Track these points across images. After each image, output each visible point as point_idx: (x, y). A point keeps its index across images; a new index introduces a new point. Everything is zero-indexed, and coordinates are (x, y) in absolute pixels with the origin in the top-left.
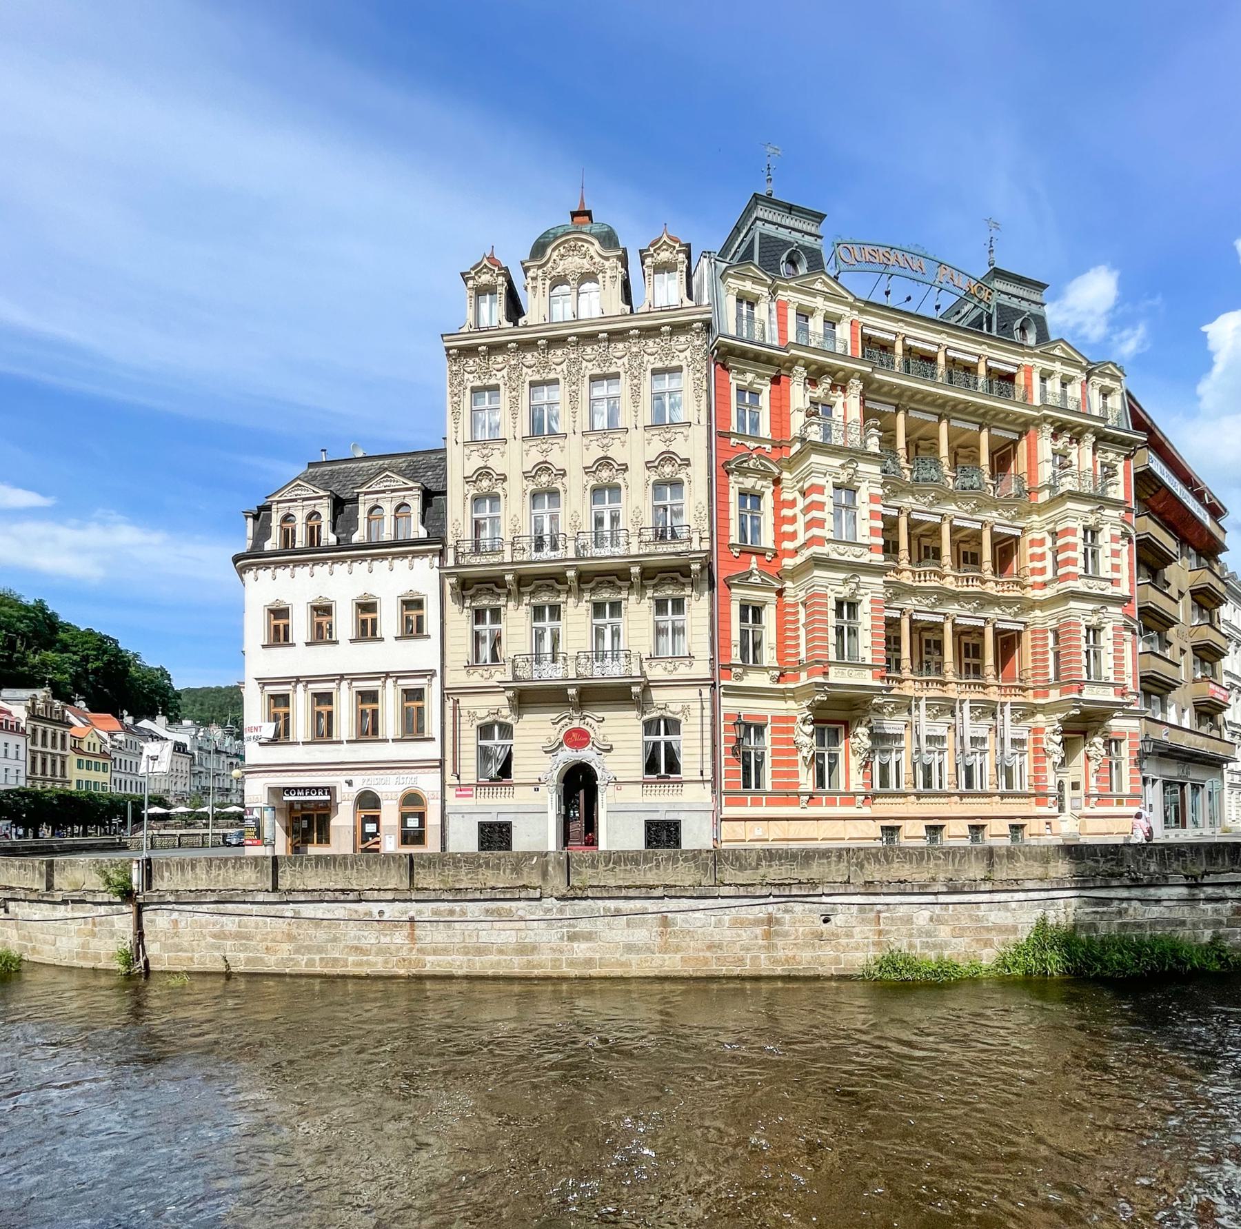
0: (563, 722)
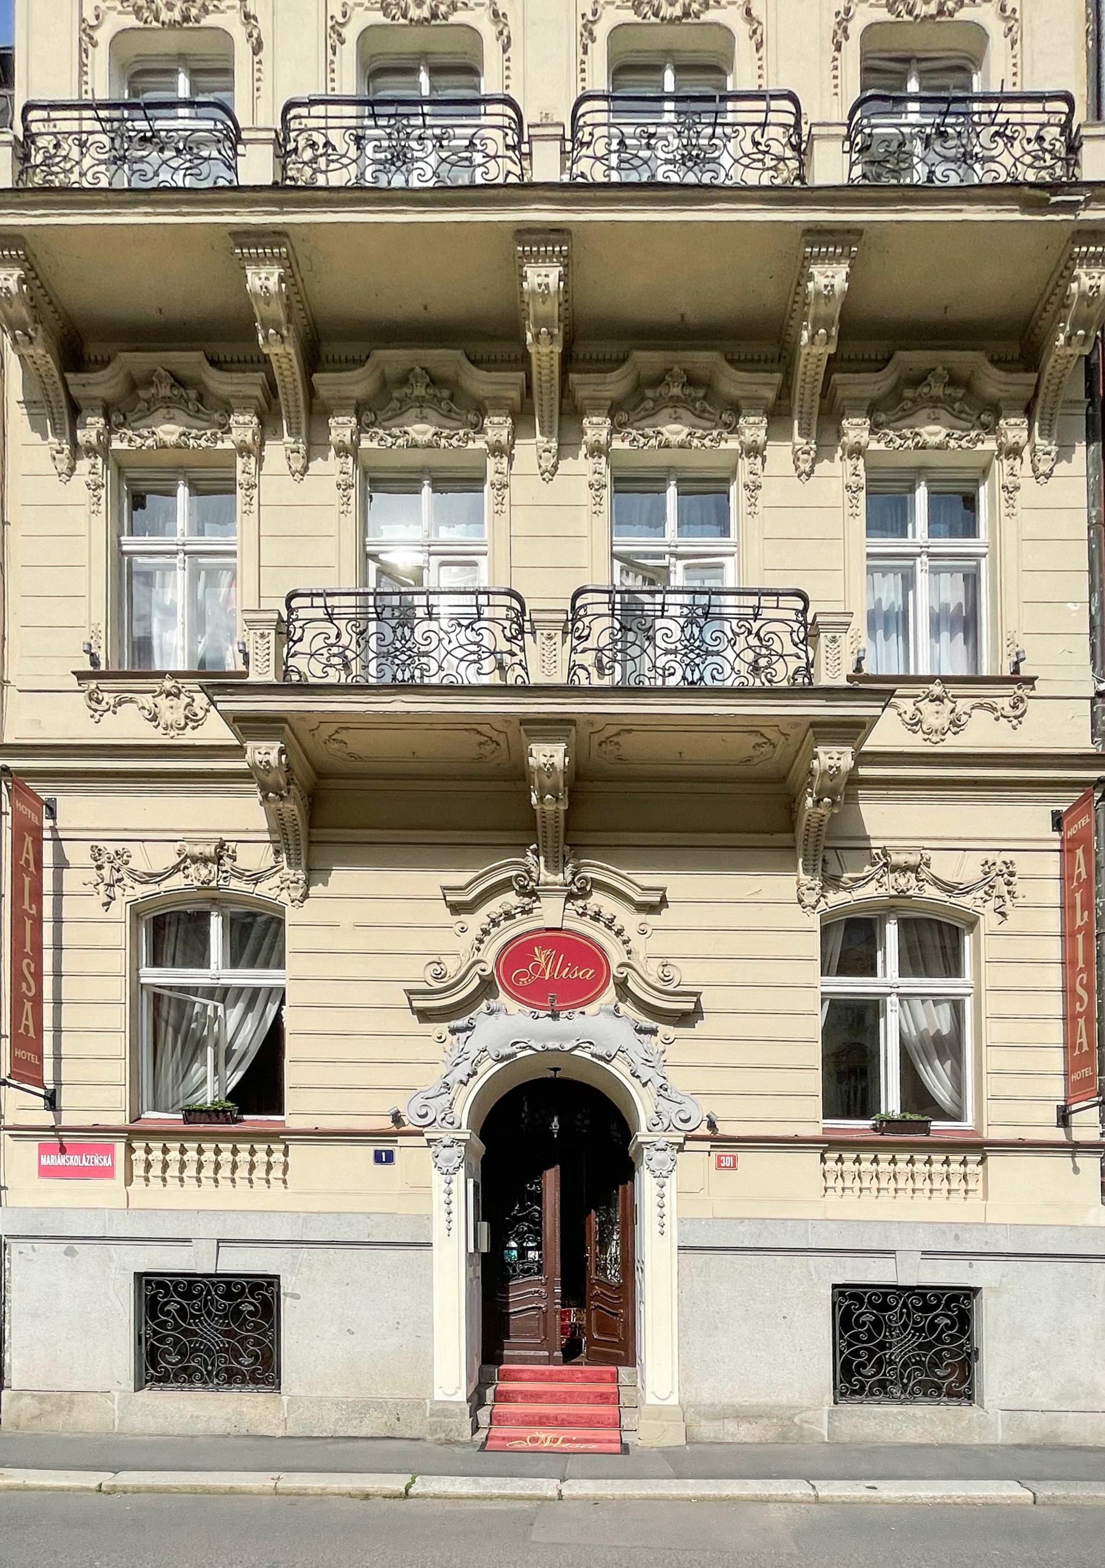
0: (494, 906)
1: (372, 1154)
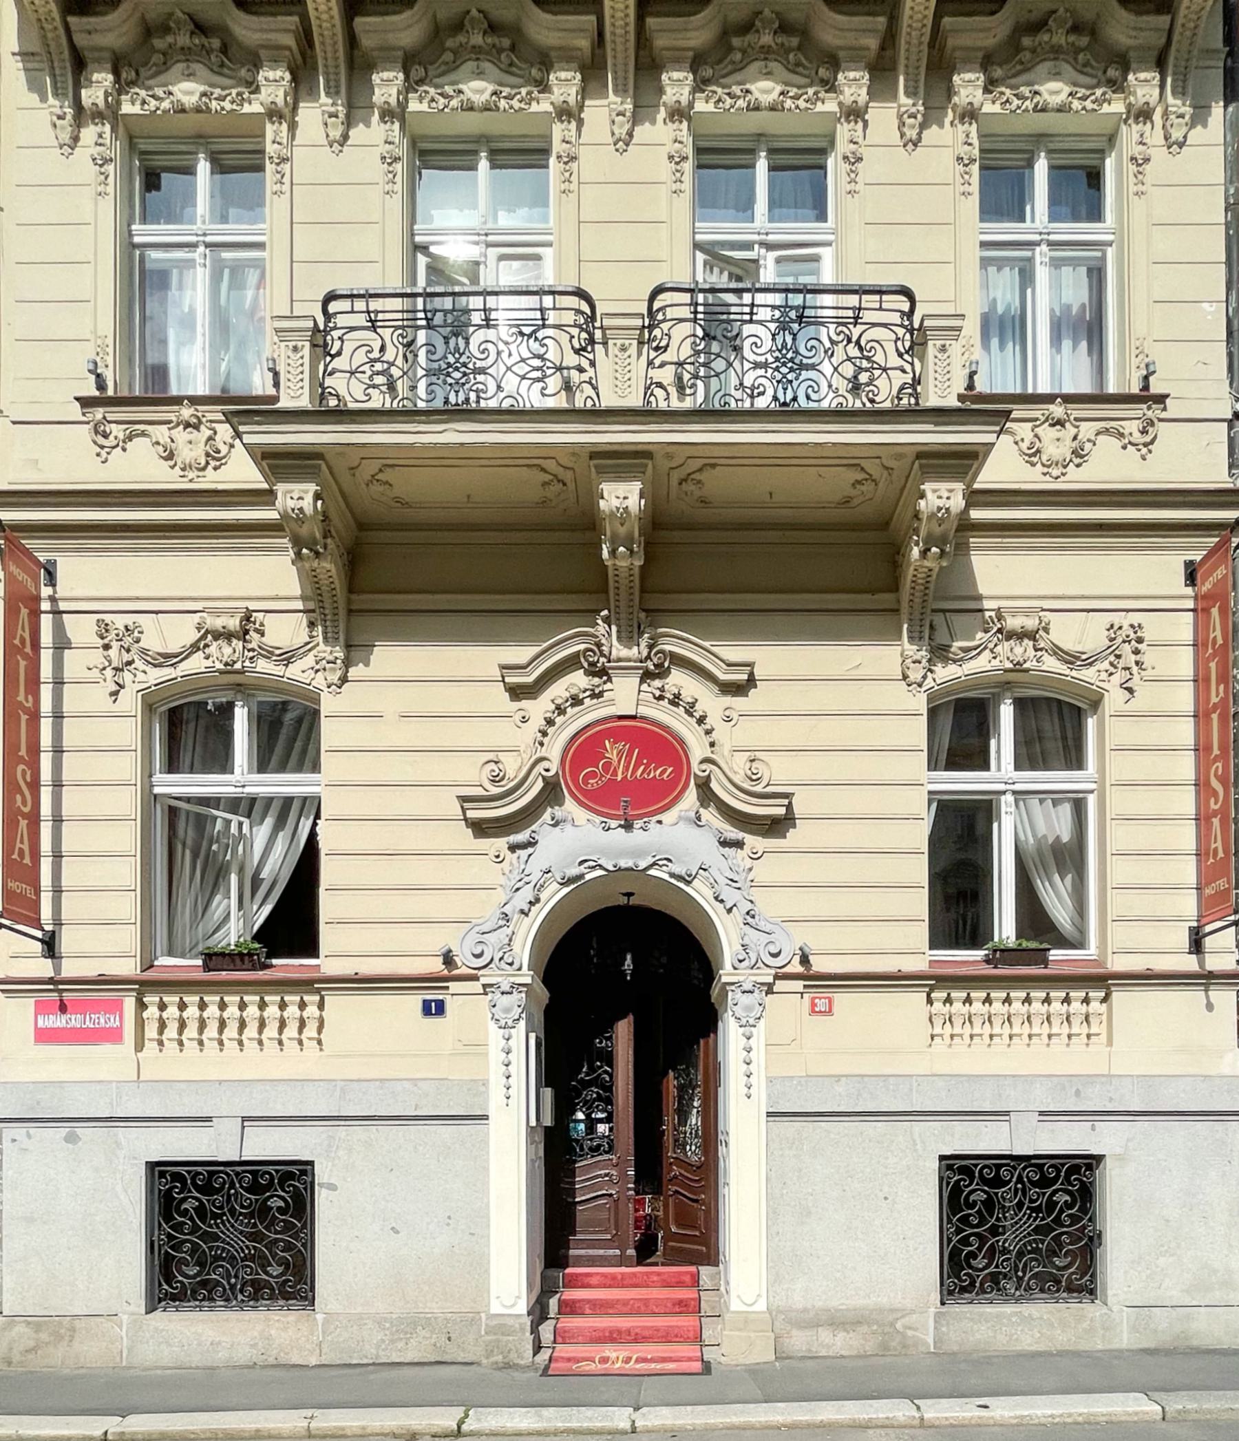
0: (559, 690)
1: (419, 1006)
